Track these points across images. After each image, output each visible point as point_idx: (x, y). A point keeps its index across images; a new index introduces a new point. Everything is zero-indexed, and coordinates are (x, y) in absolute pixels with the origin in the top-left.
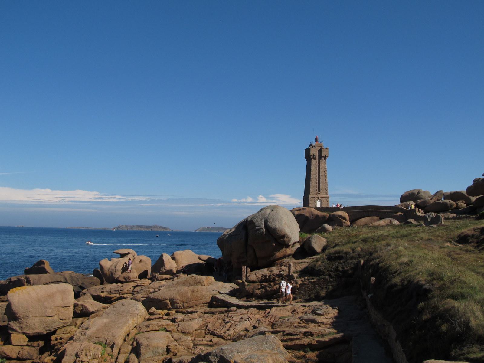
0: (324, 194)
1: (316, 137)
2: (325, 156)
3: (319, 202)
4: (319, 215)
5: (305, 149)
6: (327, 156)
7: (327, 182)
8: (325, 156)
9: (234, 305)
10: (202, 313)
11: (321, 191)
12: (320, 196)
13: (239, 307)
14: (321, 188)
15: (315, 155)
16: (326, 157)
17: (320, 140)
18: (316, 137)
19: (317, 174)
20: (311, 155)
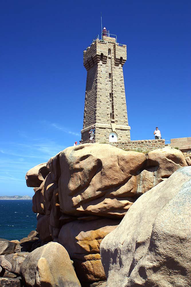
0: (120, 124)
3: (113, 136)
4: (125, 155)
12: (114, 126)
14: (115, 113)
20: (97, 53)
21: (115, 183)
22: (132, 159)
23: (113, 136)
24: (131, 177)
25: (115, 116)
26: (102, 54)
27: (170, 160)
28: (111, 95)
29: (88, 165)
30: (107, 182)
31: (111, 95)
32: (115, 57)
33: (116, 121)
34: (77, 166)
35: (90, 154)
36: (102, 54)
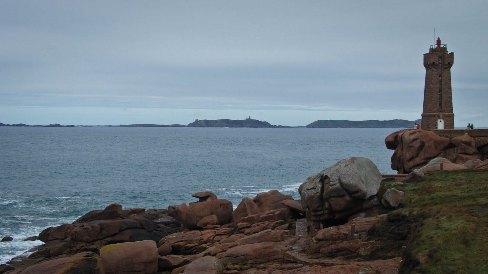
1: (439, 39)
2: (449, 63)
5: (424, 55)
6: (451, 63)
7: (451, 97)
8: (449, 63)
9: (301, 262)
10: (273, 268)
11: (443, 109)
12: (441, 115)
13: (306, 263)
14: (443, 104)
15: (435, 63)
16: (450, 64)
17: (442, 43)
18: (439, 39)
19: (438, 86)
21: (432, 156)
22: (443, 142)
23: (441, 121)
24: (441, 152)
25: (443, 107)
26: (434, 63)
27: (463, 144)
28: (440, 90)
29: (417, 144)
30: (427, 155)
31: (440, 90)
32: (444, 62)
33: (444, 110)
34: (411, 145)
35: (419, 138)
36: (434, 63)
